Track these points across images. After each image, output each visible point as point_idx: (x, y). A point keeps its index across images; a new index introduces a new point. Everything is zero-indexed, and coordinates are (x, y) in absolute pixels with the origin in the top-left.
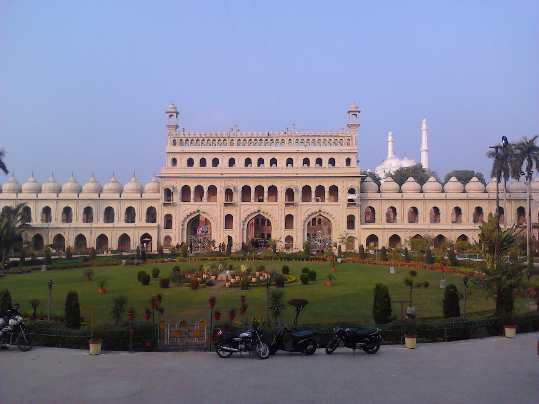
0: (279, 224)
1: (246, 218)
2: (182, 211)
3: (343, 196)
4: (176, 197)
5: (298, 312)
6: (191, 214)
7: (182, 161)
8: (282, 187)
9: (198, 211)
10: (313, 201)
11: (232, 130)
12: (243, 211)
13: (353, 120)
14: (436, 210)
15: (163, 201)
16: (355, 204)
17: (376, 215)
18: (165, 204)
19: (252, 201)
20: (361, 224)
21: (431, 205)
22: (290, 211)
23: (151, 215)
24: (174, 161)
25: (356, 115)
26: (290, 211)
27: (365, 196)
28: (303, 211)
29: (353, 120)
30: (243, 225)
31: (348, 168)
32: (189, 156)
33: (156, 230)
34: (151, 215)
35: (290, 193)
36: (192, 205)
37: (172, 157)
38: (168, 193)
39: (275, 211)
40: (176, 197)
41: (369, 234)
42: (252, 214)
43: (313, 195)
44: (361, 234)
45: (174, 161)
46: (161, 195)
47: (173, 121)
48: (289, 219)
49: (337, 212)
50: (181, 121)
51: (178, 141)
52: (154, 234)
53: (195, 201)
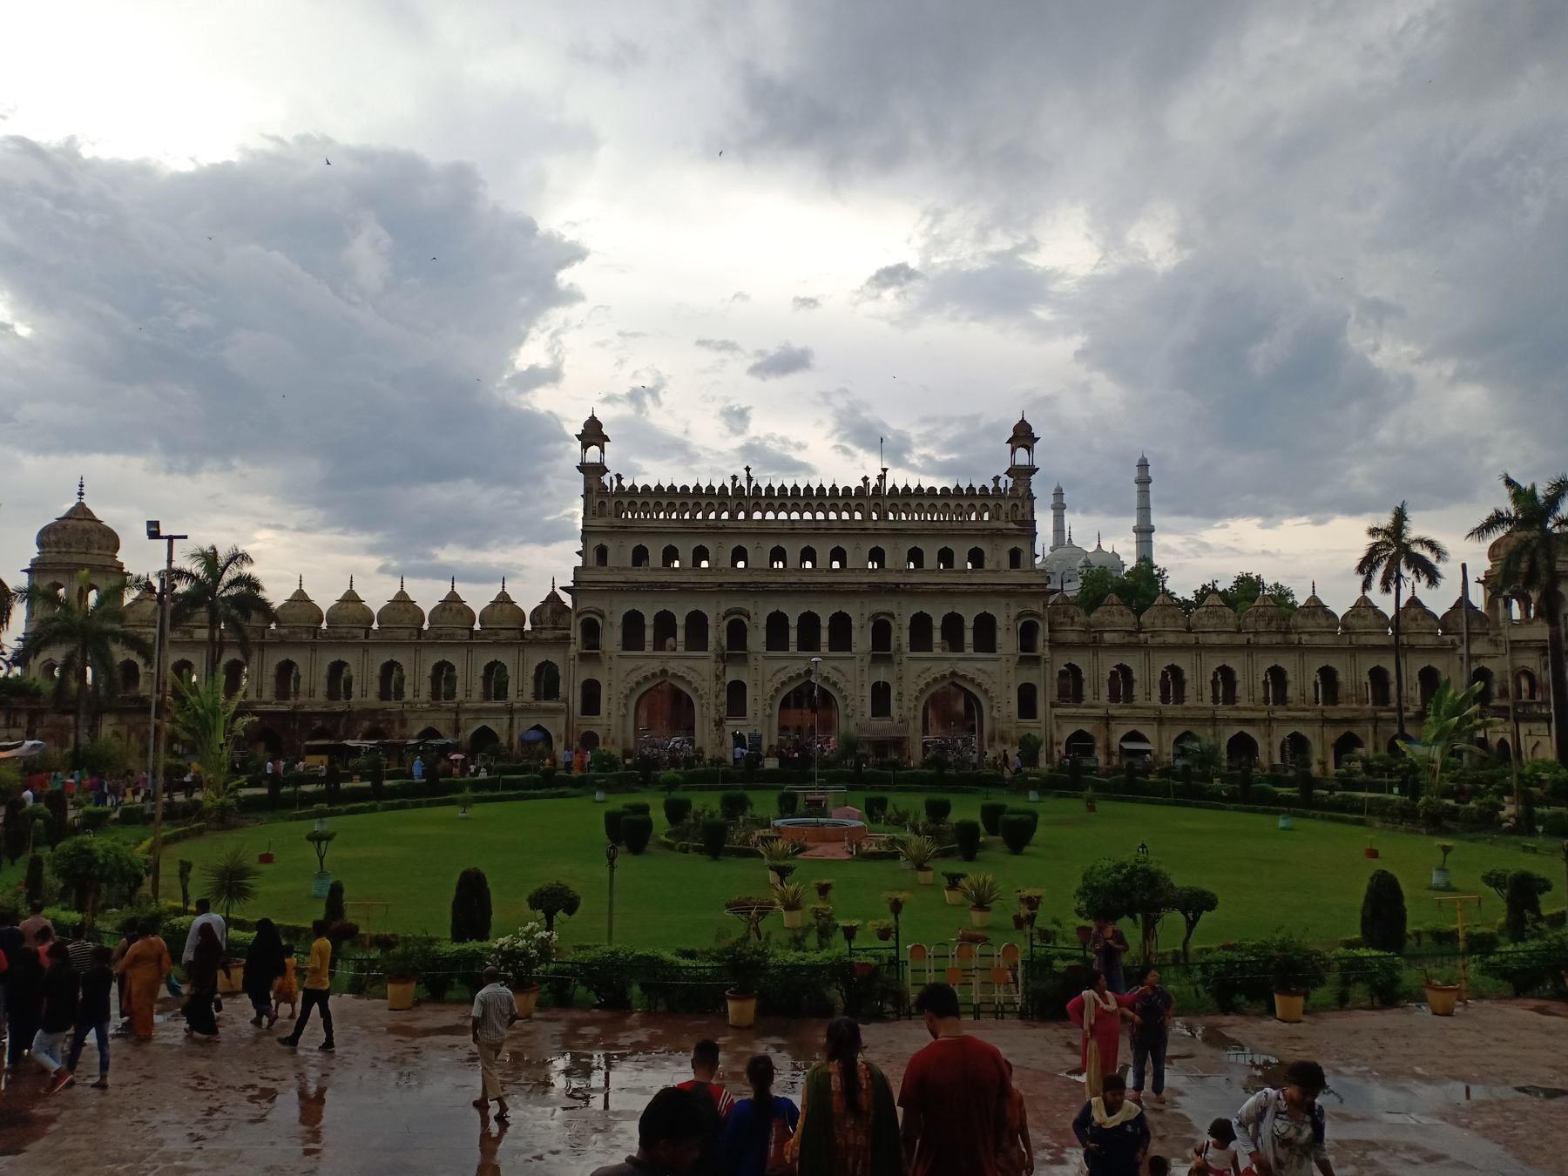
0: (858, 700)
1: (777, 690)
2: (622, 672)
3: (1007, 641)
4: (612, 638)
5: (1191, 925)
6: (646, 678)
7: (620, 553)
8: (860, 615)
9: (664, 672)
10: (937, 652)
11: (734, 478)
12: (768, 674)
13: (1022, 457)
14: (1226, 673)
15: (576, 647)
16: (1037, 660)
17: (1085, 685)
18: (582, 657)
19: (793, 649)
20: (1053, 705)
21: (1214, 662)
22: (882, 674)
23: (547, 681)
24: (602, 553)
25: (1029, 449)
26: (882, 674)
27: (1059, 637)
28: (915, 674)
29: (1022, 457)
30: (771, 706)
31: (1014, 572)
32: (635, 543)
33: (562, 720)
34: (547, 681)
35: (881, 632)
36: (647, 657)
37: (595, 542)
38: (591, 631)
39: (849, 676)
40: (612, 638)
41: (1069, 730)
42: (791, 678)
43: (937, 636)
44: (1054, 726)
45: (602, 553)
46: (576, 633)
47: (593, 454)
48: (881, 695)
49: (996, 676)
50: (613, 456)
51: (610, 504)
52: (556, 727)
53: (687, 649)
